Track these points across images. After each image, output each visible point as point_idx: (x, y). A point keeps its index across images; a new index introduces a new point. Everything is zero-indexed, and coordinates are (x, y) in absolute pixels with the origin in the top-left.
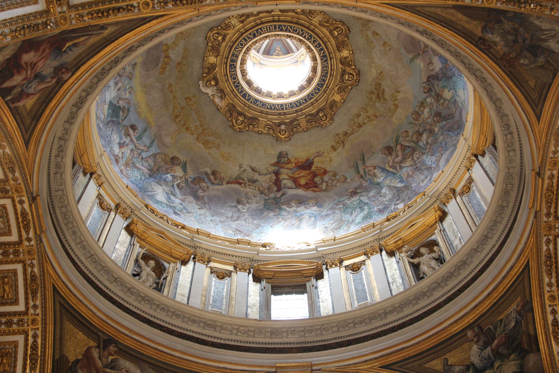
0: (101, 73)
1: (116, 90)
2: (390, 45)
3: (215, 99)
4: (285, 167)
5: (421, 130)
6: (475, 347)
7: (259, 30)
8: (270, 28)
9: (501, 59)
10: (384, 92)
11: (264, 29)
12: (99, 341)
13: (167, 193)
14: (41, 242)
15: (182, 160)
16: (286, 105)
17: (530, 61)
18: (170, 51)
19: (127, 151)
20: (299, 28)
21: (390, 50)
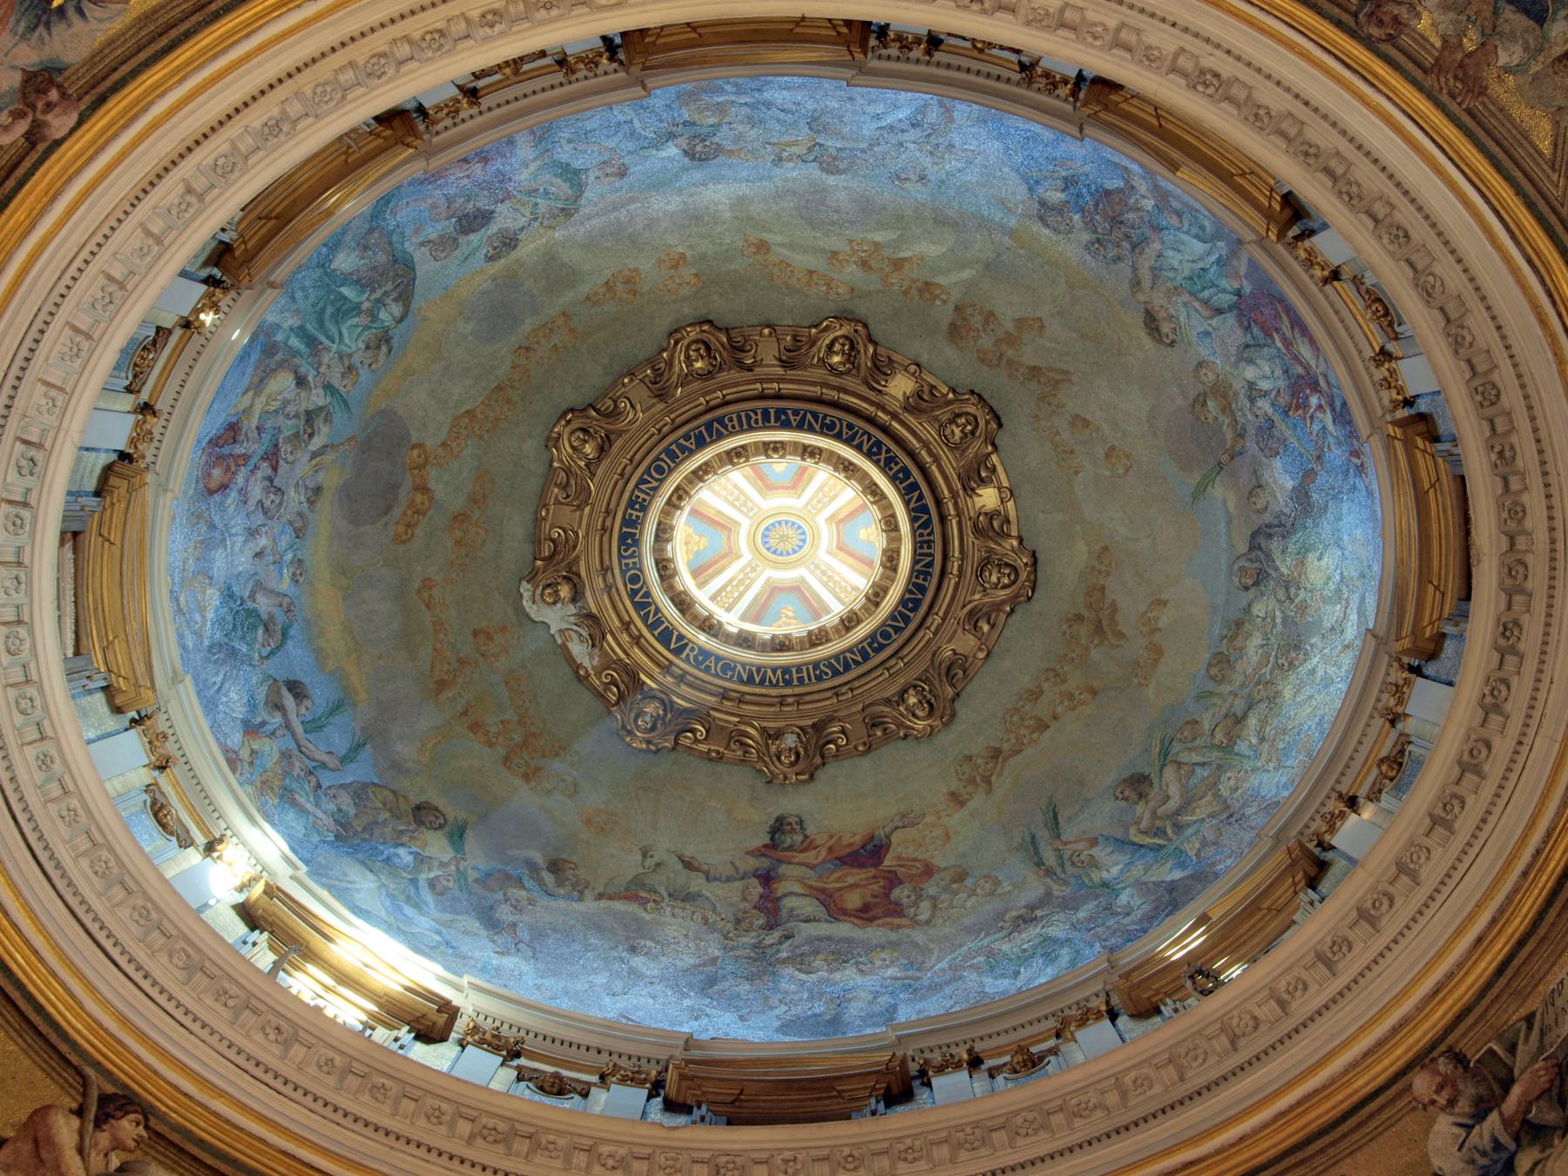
2: (1128, 456)
3: (570, 645)
4: (796, 860)
5: (1239, 705)
6: (1444, 1126)
8: (749, 418)
9: (1438, 67)
10: (1115, 610)
11: (731, 420)
12: (84, 1095)
13: (392, 896)
15: (451, 819)
16: (799, 670)
17: (1526, 49)
18: (432, 472)
19: (270, 749)
20: (839, 420)
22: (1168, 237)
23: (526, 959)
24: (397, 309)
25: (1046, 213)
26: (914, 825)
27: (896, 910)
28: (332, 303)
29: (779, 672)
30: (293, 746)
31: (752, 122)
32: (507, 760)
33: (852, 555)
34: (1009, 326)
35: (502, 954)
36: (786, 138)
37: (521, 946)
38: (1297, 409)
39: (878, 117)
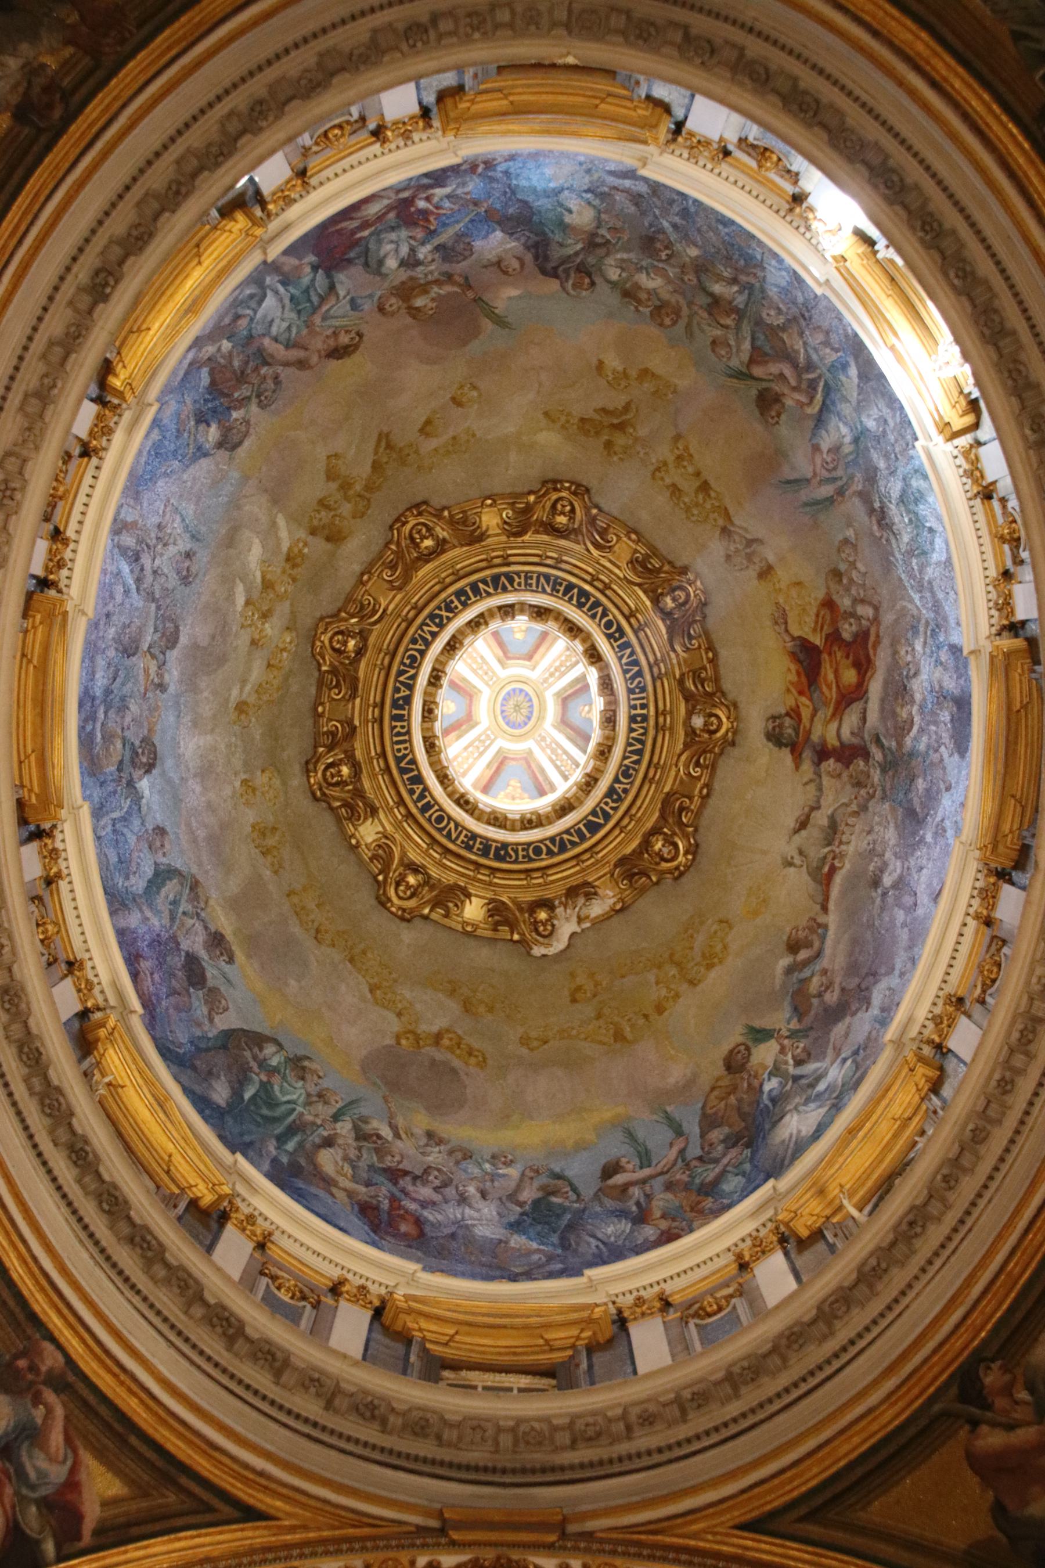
0: (142, 1248)
1: (481, 1204)
2: (461, 387)
3: (593, 915)
4: (808, 725)
5: (703, 300)
7: (402, 765)
8: (399, 734)
10: (604, 410)
11: (399, 750)
13: (806, 1102)
14: (589, 1535)
15: (740, 1039)
18: (423, 1028)
20: (407, 650)
21: (474, 387)
22: (259, 329)
23: (875, 983)
24: (270, 1049)
25: (228, 443)
26: (784, 614)
27: (862, 637)
28: (259, 1108)
29: (634, 726)
30: (661, 1179)
31: (123, 708)
32: (693, 983)
33: (538, 647)
34: (333, 486)
35: (869, 1004)
36: (141, 677)
37: (863, 986)
38: (428, 221)
39: (127, 592)
